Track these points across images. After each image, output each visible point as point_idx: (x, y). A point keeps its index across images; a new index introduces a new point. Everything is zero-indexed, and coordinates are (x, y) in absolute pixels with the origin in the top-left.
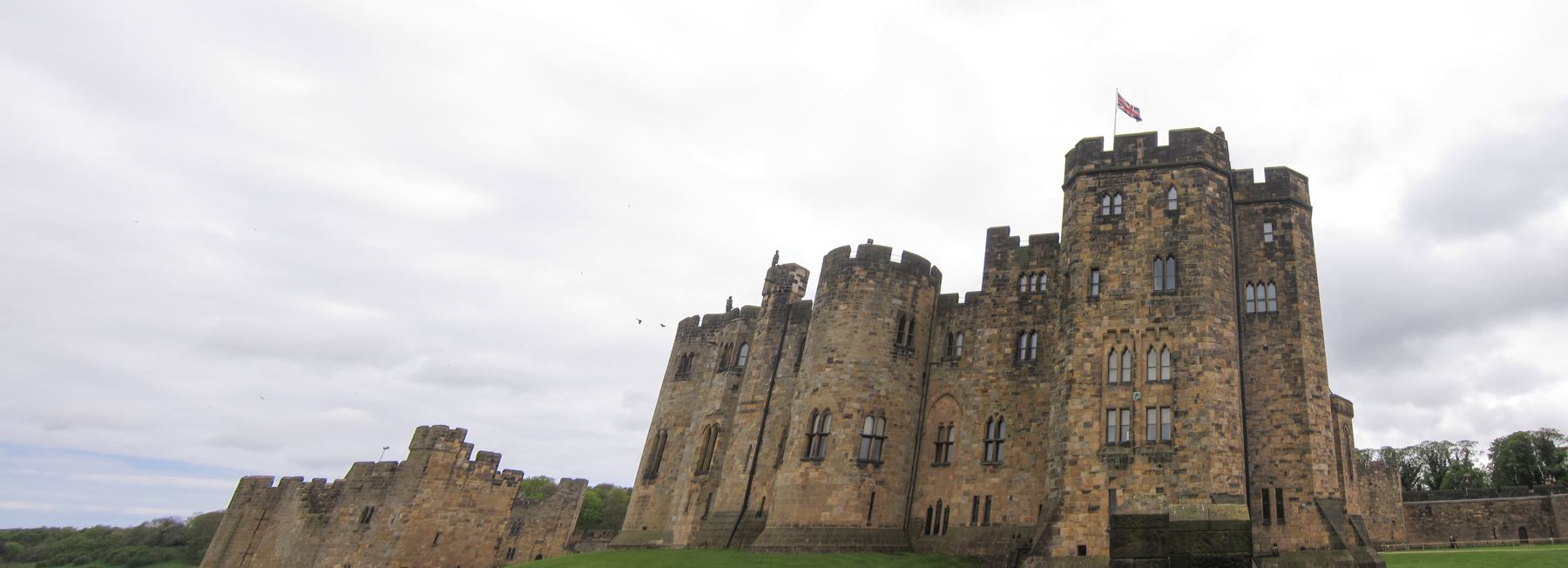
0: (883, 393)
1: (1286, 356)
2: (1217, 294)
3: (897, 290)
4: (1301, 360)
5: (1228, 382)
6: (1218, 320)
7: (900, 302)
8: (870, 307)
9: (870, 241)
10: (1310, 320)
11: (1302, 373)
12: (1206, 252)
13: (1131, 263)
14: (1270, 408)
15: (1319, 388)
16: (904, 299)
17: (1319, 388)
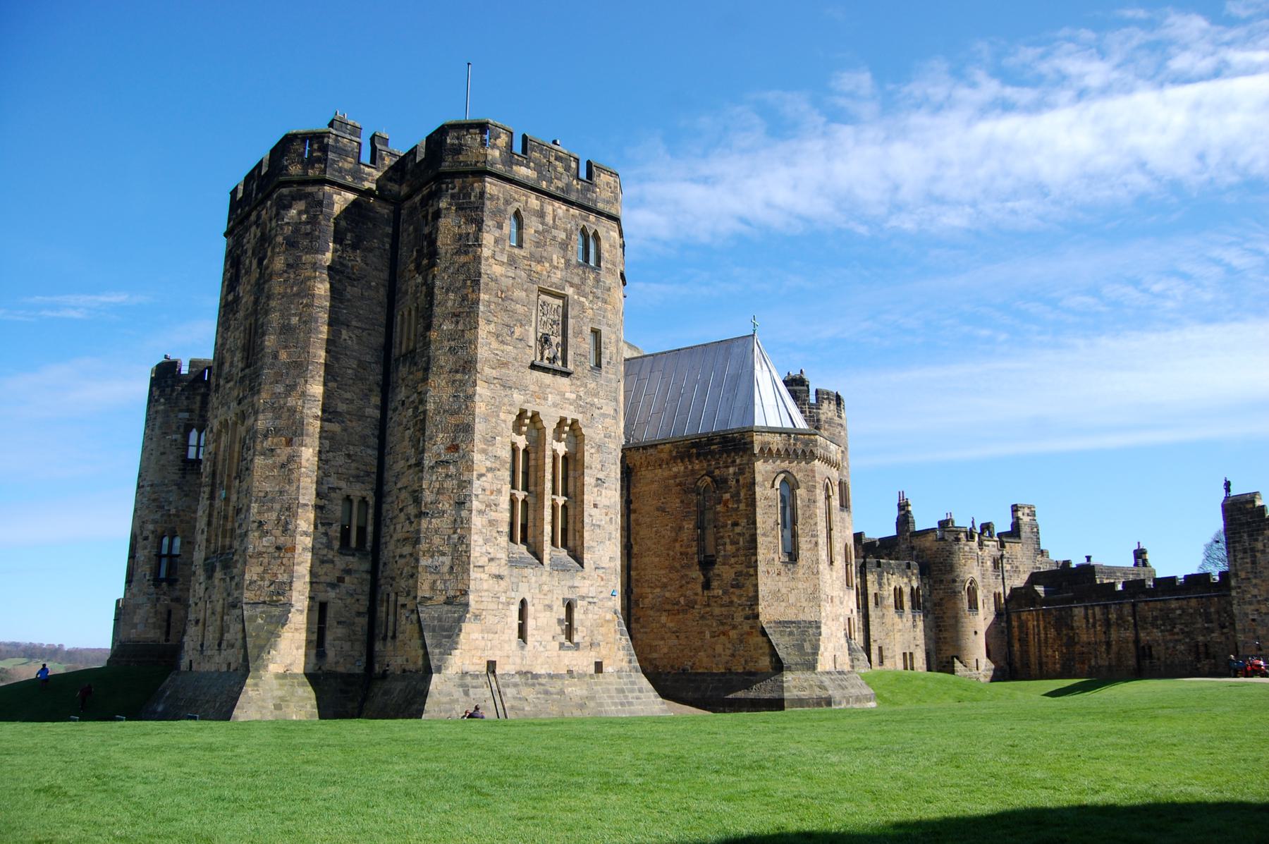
0: (173, 511)
1: (416, 408)
2: (283, 356)
3: (184, 402)
4: (425, 412)
5: (283, 466)
6: (280, 389)
7: (186, 415)
8: (160, 428)
9: (166, 357)
10: (452, 350)
11: (423, 430)
12: (273, 303)
13: (237, 333)
14: (399, 485)
15: (454, 448)
16: (190, 411)
17: (454, 448)
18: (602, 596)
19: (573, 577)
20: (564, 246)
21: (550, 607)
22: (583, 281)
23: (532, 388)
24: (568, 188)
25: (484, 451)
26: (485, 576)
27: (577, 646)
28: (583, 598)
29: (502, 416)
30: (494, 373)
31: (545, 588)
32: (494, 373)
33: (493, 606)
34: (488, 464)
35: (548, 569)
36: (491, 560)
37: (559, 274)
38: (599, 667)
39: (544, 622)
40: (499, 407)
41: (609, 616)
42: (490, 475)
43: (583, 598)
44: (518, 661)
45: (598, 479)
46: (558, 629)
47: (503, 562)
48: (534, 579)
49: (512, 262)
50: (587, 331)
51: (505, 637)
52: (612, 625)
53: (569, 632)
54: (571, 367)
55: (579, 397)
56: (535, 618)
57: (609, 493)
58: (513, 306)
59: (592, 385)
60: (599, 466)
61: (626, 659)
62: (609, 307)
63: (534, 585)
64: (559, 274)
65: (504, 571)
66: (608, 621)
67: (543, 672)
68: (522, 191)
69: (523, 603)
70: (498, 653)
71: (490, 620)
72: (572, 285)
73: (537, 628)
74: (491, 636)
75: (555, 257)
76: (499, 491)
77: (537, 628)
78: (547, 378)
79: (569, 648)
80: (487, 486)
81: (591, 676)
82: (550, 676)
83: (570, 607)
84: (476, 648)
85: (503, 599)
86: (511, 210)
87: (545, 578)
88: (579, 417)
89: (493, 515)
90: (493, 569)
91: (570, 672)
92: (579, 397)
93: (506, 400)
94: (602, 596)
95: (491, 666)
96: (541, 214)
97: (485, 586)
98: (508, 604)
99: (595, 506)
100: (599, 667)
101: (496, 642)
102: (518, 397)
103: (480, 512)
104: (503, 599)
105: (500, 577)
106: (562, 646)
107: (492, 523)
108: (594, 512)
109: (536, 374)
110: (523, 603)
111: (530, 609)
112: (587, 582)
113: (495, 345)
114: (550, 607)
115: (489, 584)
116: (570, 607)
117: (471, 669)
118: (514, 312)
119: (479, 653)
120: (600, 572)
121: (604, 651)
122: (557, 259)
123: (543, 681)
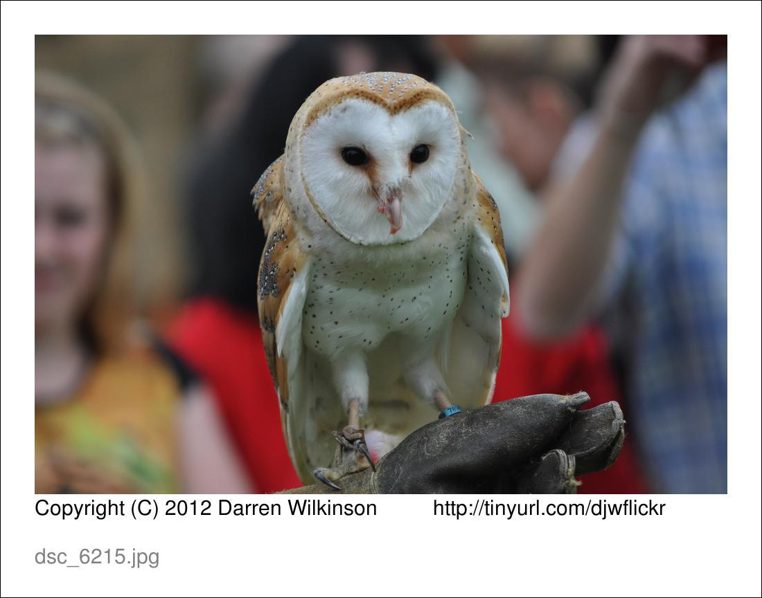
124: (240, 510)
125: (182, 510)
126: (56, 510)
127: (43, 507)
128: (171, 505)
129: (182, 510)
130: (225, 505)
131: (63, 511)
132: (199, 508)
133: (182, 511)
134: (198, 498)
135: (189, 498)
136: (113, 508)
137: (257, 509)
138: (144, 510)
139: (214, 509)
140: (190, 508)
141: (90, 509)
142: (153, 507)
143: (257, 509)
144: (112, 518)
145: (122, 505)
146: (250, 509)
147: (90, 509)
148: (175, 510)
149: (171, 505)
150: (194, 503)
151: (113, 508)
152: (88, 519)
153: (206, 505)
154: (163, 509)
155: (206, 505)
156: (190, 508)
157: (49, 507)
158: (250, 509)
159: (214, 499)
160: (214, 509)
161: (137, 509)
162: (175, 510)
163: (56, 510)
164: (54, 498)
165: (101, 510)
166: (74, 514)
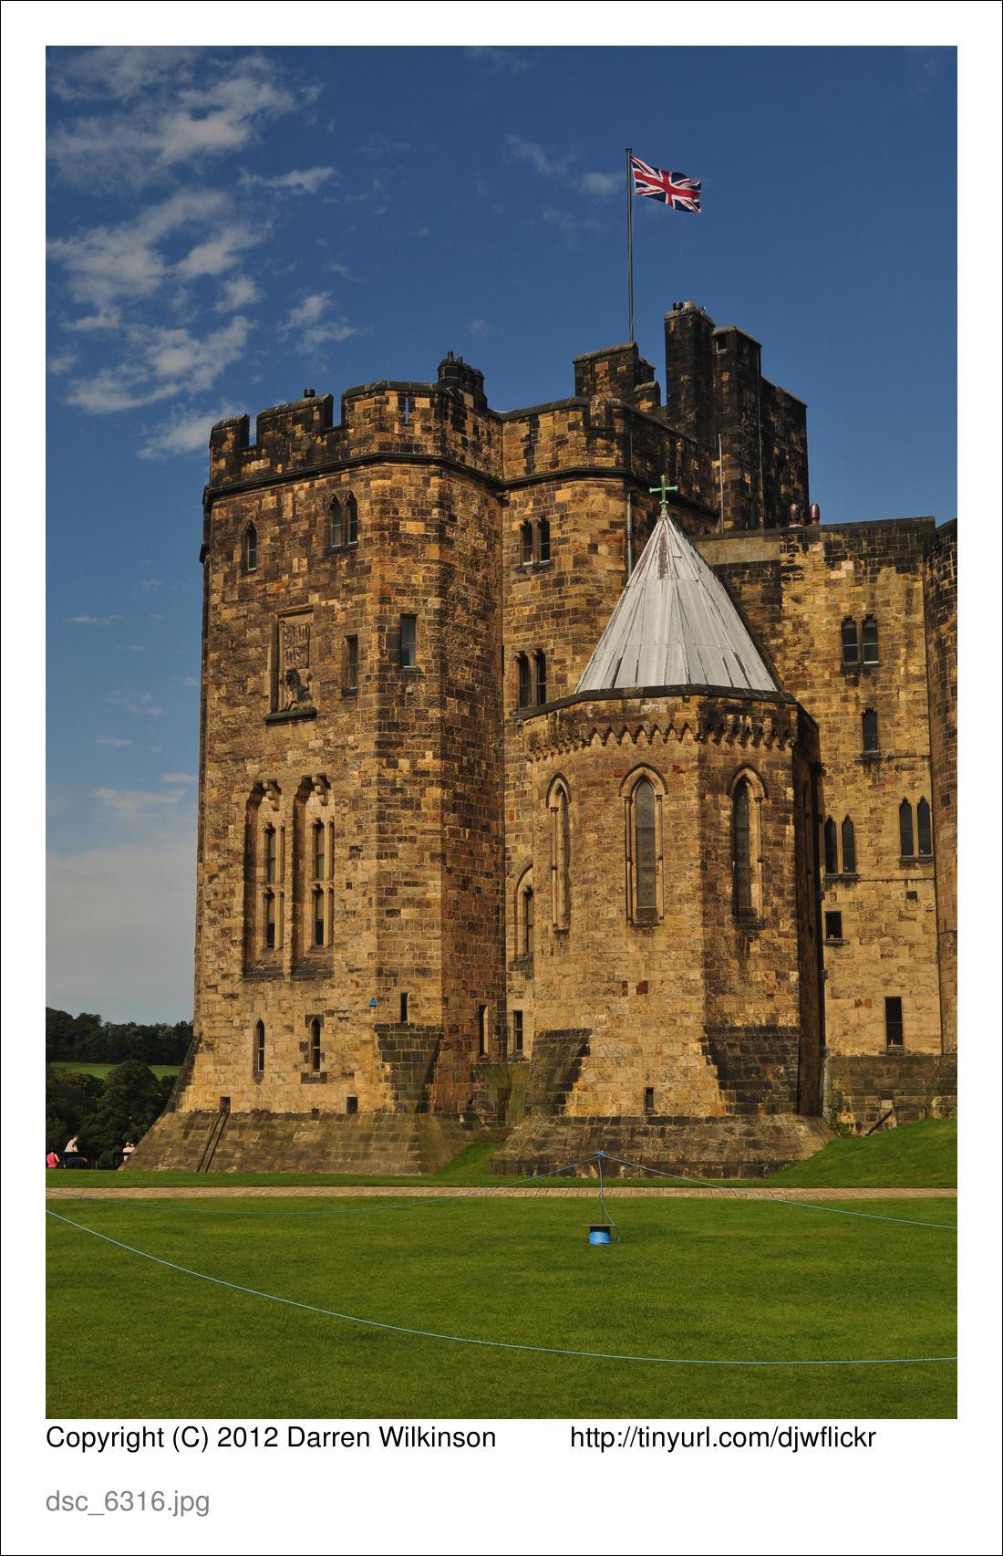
18: (358, 1008)
19: (318, 986)
20: (306, 541)
21: (290, 1029)
22: (332, 574)
23: (269, 750)
24: (311, 452)
25: (216, 847)
26: (217, 997)
27: (324, 1078)
28: (331, 1013)
29: (235, 798)
30: (225, 747)
31: (285, 1004)
32: (225, 747)
33: (225, 1032)
34: (221, 862)
35: (288, 980)
36: (224, 977)
37: (300, 582)
38: (352, 1103)
39: (285, 1046)
40: (231, 788)
41: (366, 1035)
42: (222, 875)
43: (331, 1013)
44: (253, 1097)
45: (352, 848)
46: (300, 1056)
47: (237, 977)
48: (270, 994)
49: (245, 595)
50: (338, 643)
51: (239, 1068)
52: (370, 1047)
53: (317, 1058)
54: (317, 704)
55: (327, 742)
56: (273, 1044)
57: (367, 863)
58: (242, 653)
59: (344, 718)
60: (355, 829)
61: (390, 1093)
62: (369, 596)
63: (271, 1002)
64: (300, 582)
65: (238, 989)
66: (365, 1042)
67: (281, 1111)
68: (253, 494)
69: (260, 1026)
70: (231, 1087)
71: (224, 1048)
72: (316, 589)
73: (276, 1057)
74: (224, 1068)
75: (295, 561)
76: (232, 892)
77: (276, 1057)
78: (286, 731)
79: (314, 1080)
80: (219, 888)
81: (340, 1117)
82: (289, 1116)
83: (316, 1024)
84: (209, 1083)
85: (237, 1023)
86: (242, 528)
87: (285, 992)
88: (327, 769)
89: (227, 922)
90: (226, 987)
91: (315, 1111)
92: (327, 742)
93: (239, 776)
94: (358, 1008)
95: (226, 1100)
96: (279, 511)
97: (218, 1010)
98: (242, 1028)
99: (349, 886)
100: (352, 1103)
101: (229, 1075)
102: (252, 768)
103: (213, 921)
104: (237, 1023)
105: (233, 996)
106: (305, 1078)
107: (225, 932)
108: (348, 894)
109: (277, 730)
110: (260, 1026)
111: (268, 1032)
112: (337, 991)
113: (225, 711)
114: (290, 1029)
115: (222, 1006)
116: (316, 1024)
117: (204, 1106)
118: (247, 660)
119: (212, 1089)
120: (354, 976)
121: (359, 1083)
122: (299, 564)
123: (276, 1122)
124: (316, 1441)
125: (240, 1440)
126: (73, 1439)
127: (56, 1437)
128: (225, 1433)
129: (240, 1440)
130: (296, 1433)
131: (83, 1441)
132: (262, 1438)
133: (240, 1441)
134: (262, 1424)
135: (249, 1424)
136: (149, 1437)
137: (338, 1438)
138: (190, 1441)
139: (282, 1439)
140: (251, 1437)
141: (118, 1438)
142: (201, 1436)
143: (338, 1438)
144: (147, 1451)
145: (160, 1433)
146: (330, 1438)
147: (118, 1438)
148: (230, 1440)
149: (225, 1433)
150: (255, 1431)
151: (149, 1437)
152: (116, 1452)
153: (272, 1433)
154: (214, 1438)
155: (272, 1433)
156: (251, 1437)
157: (64, 1436)
158: (330, 1438)
159: (282, 1425)
160: (282, 1439)
161: (181, 1439)
162: (230, 1440)
163: (73, 1439)
164: (70, 1425)
165: (133, 1440)
166: (98, 1445)
